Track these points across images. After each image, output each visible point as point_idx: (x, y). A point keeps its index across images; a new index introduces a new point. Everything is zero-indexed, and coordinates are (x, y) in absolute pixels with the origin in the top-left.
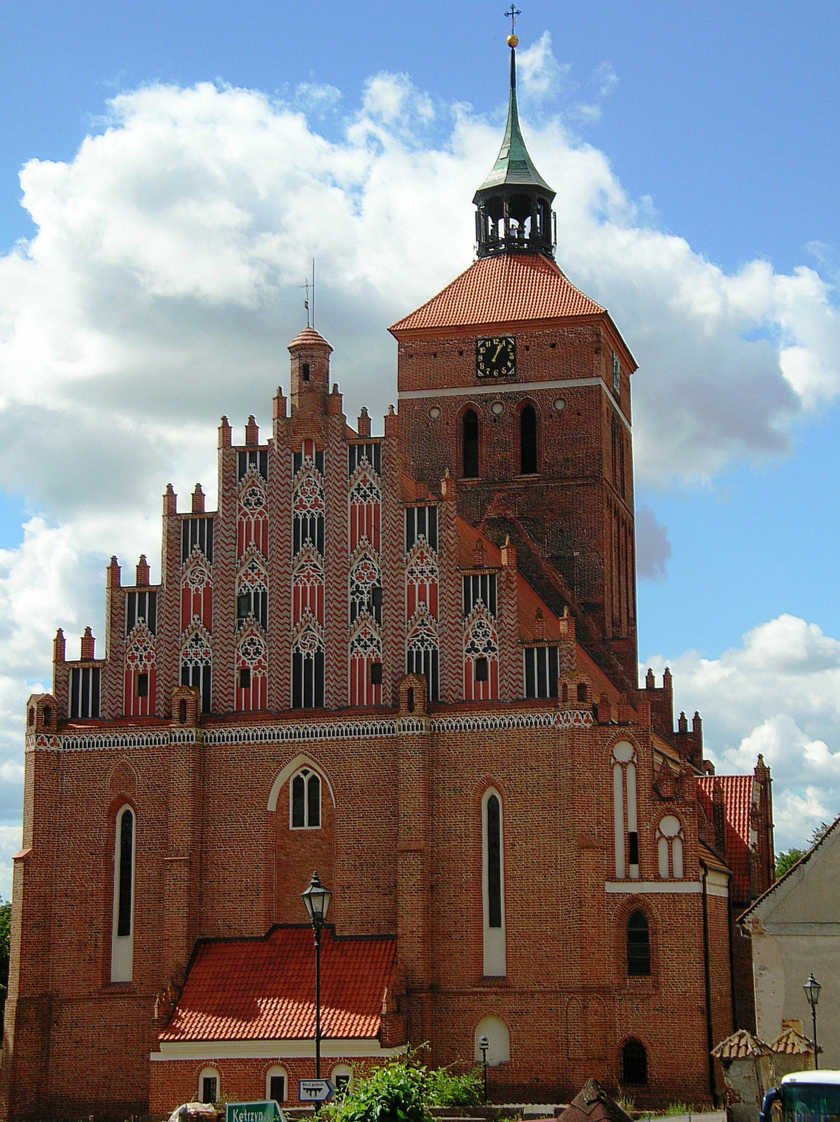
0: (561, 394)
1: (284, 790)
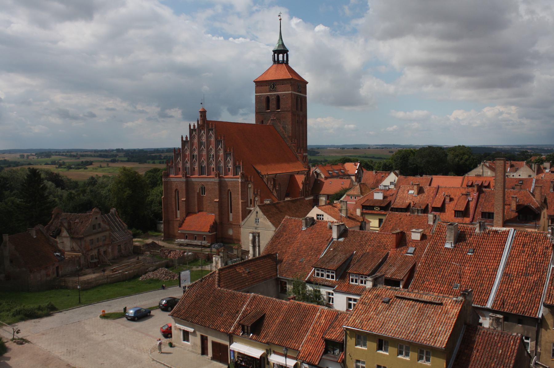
0: (284, 95)
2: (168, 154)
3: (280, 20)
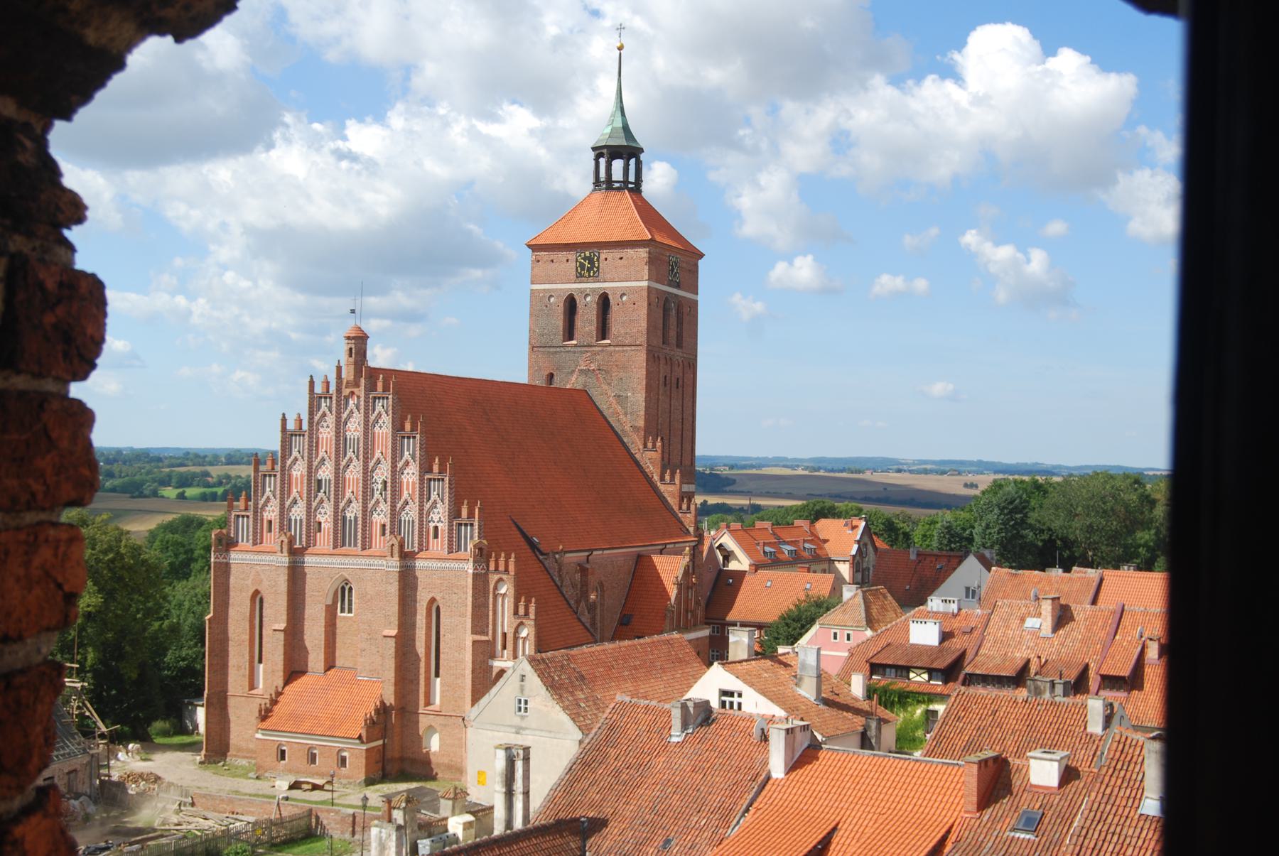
1: (336, 593)
2: (234, 470)
3: (620, 48)
